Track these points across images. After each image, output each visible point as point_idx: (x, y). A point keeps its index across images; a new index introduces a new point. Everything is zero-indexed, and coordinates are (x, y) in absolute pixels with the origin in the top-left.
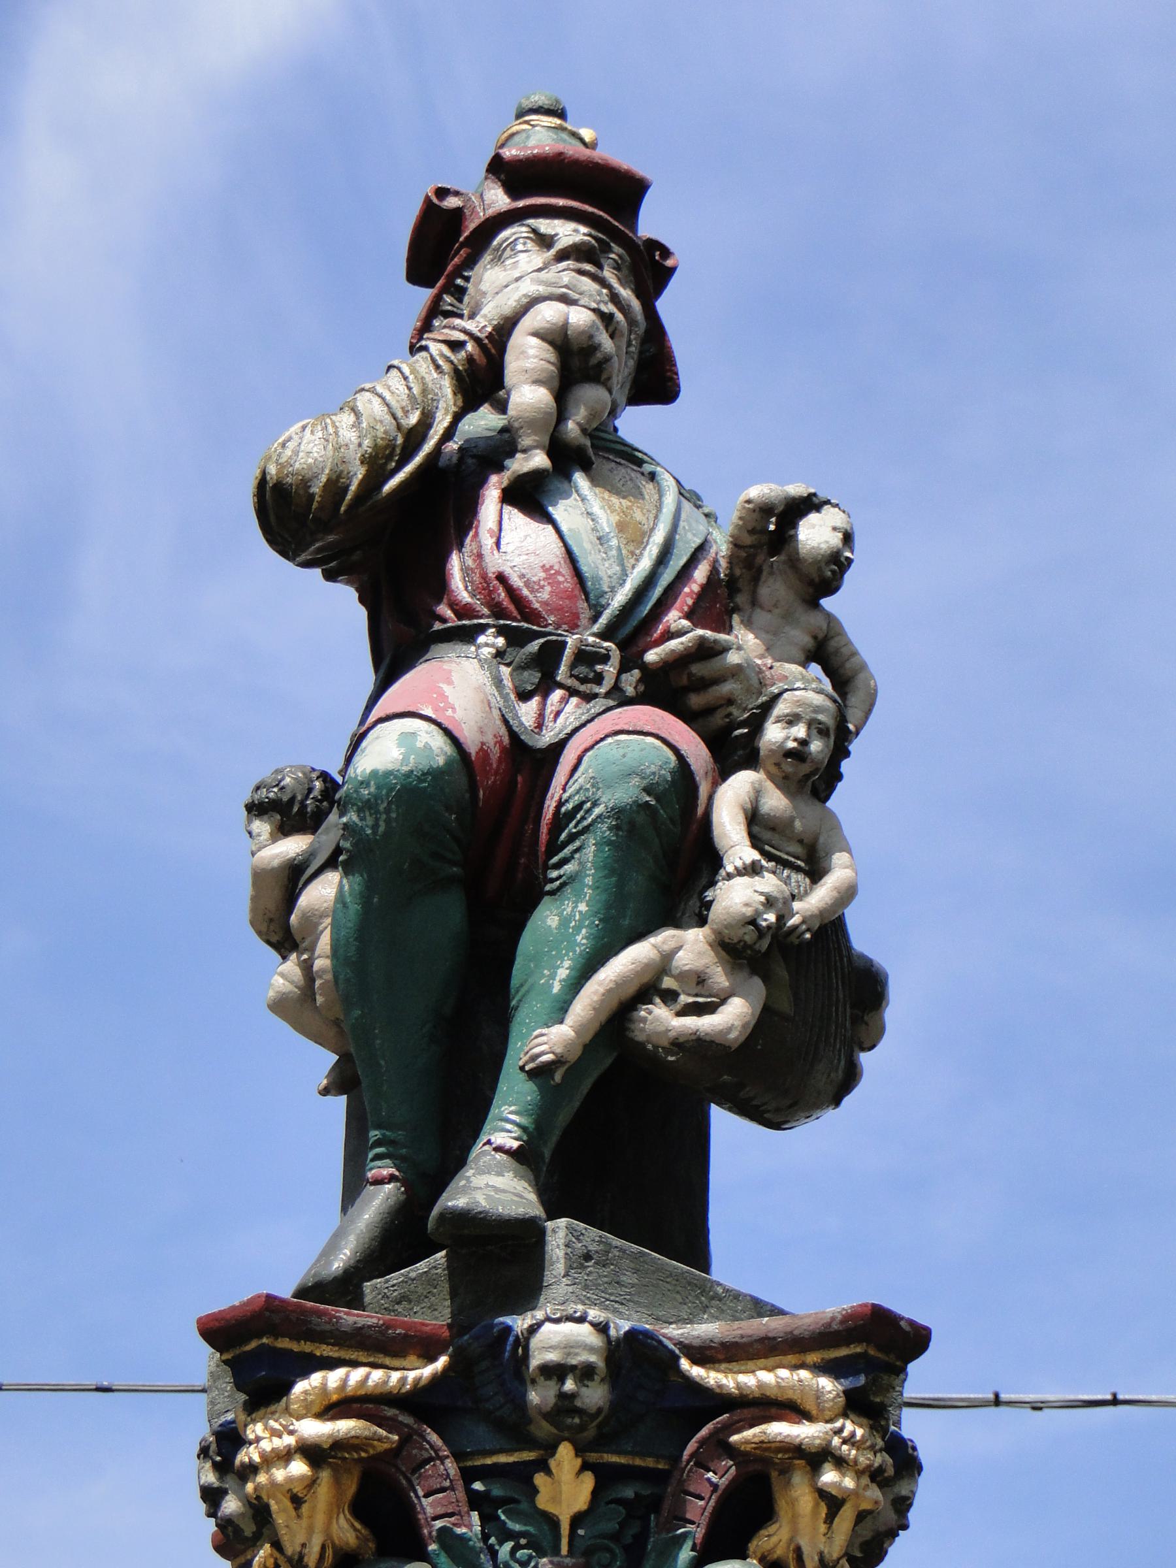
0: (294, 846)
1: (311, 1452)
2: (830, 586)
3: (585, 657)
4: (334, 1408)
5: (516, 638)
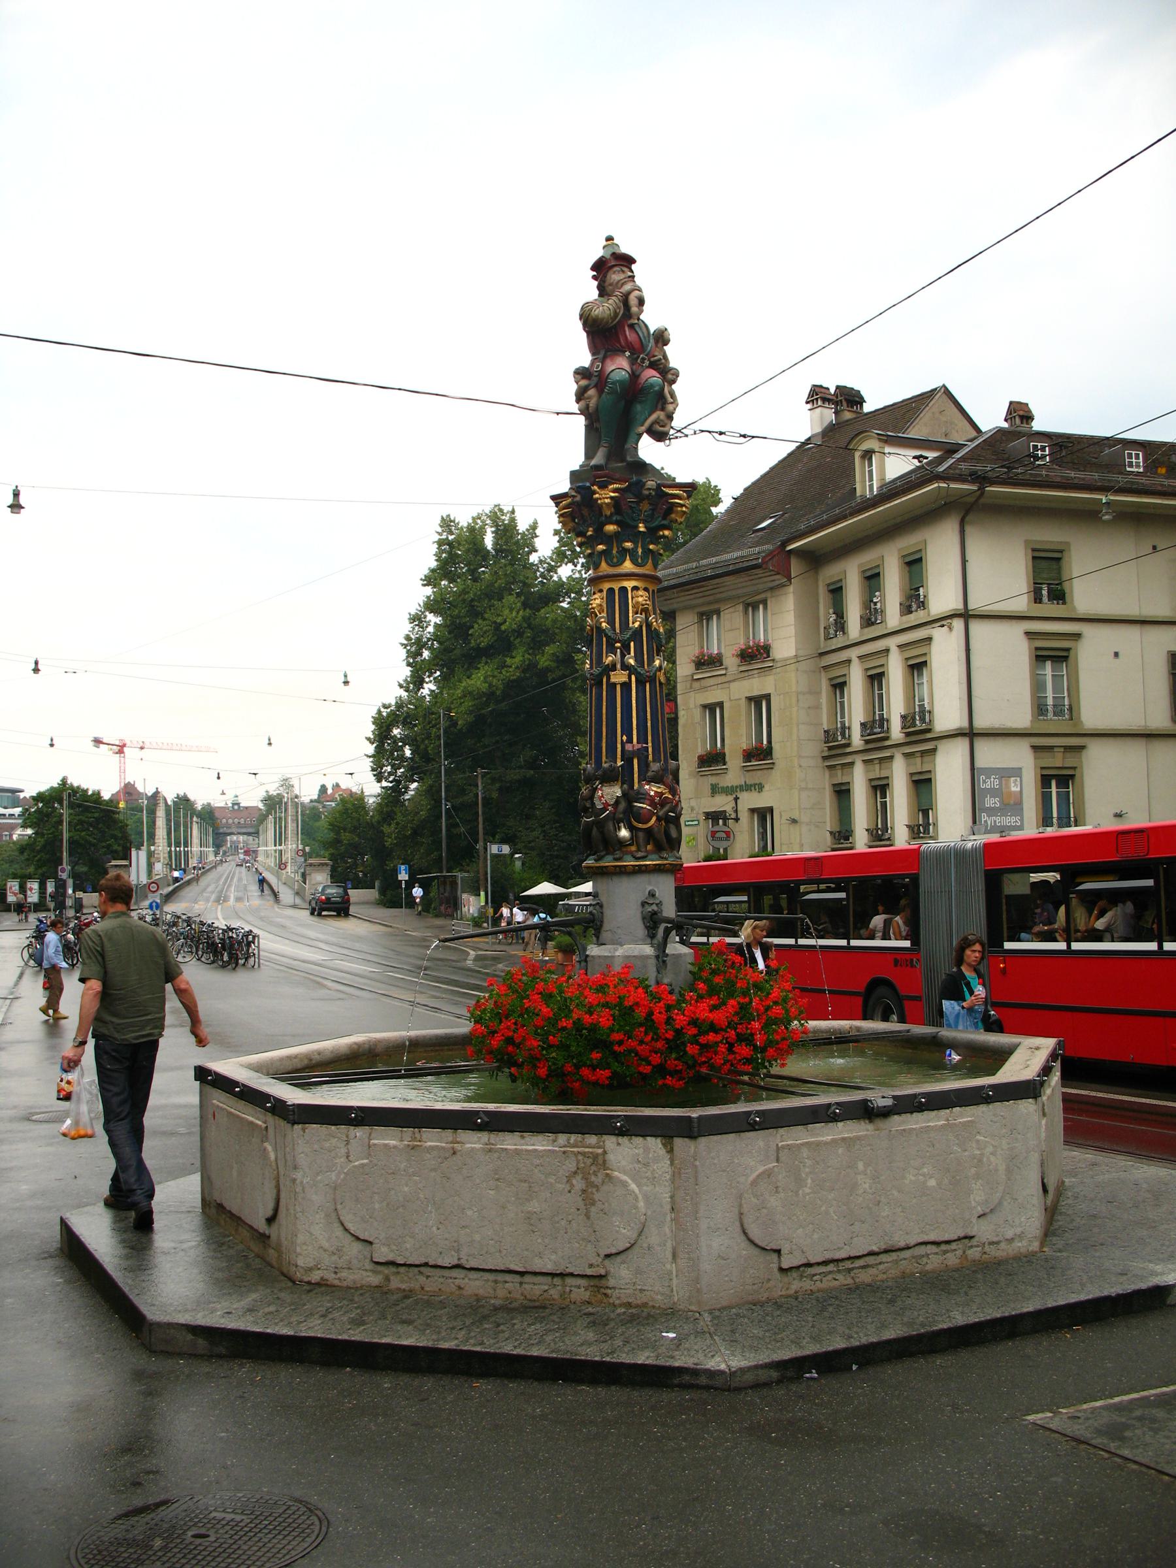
0: (584, 383)
1: (611, 498)
2: (666, 345)
3: (643, 359)
4: (614, 491)
5: (632, 354)
